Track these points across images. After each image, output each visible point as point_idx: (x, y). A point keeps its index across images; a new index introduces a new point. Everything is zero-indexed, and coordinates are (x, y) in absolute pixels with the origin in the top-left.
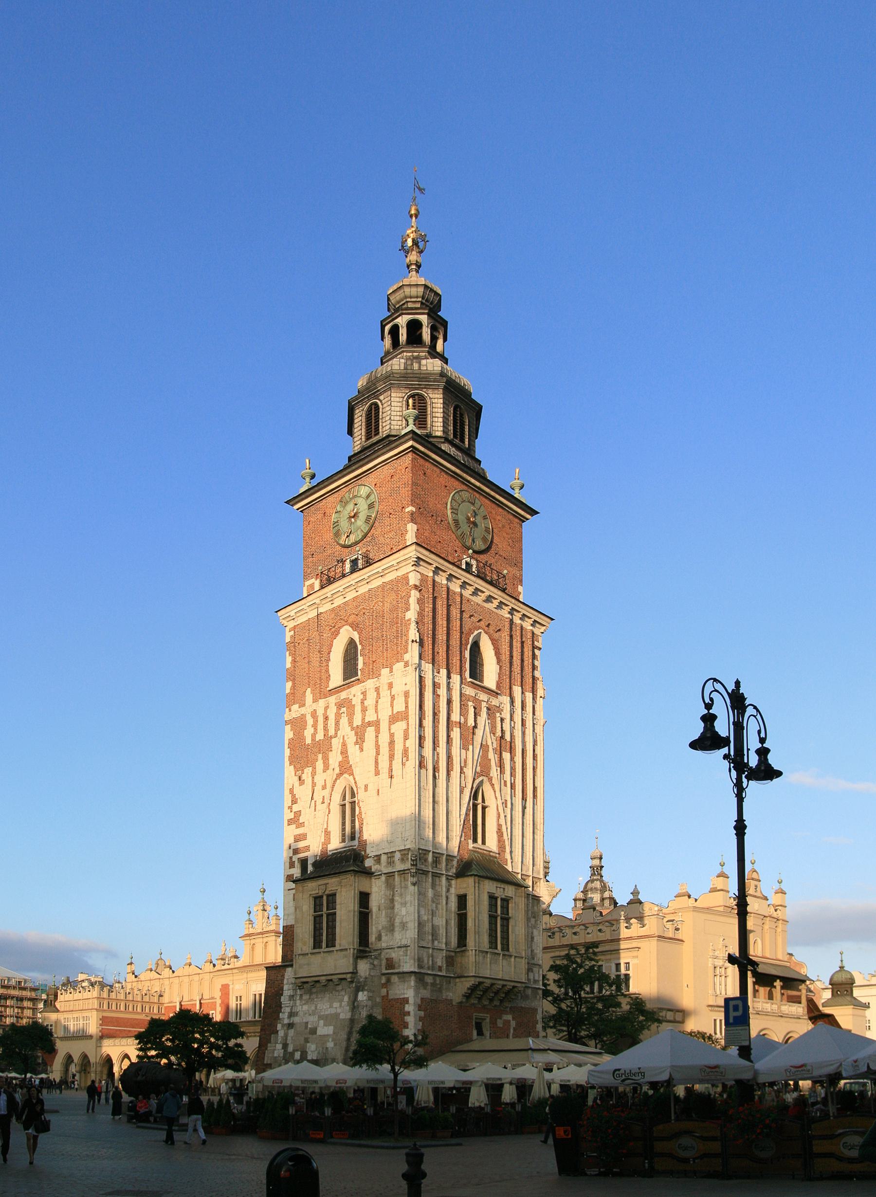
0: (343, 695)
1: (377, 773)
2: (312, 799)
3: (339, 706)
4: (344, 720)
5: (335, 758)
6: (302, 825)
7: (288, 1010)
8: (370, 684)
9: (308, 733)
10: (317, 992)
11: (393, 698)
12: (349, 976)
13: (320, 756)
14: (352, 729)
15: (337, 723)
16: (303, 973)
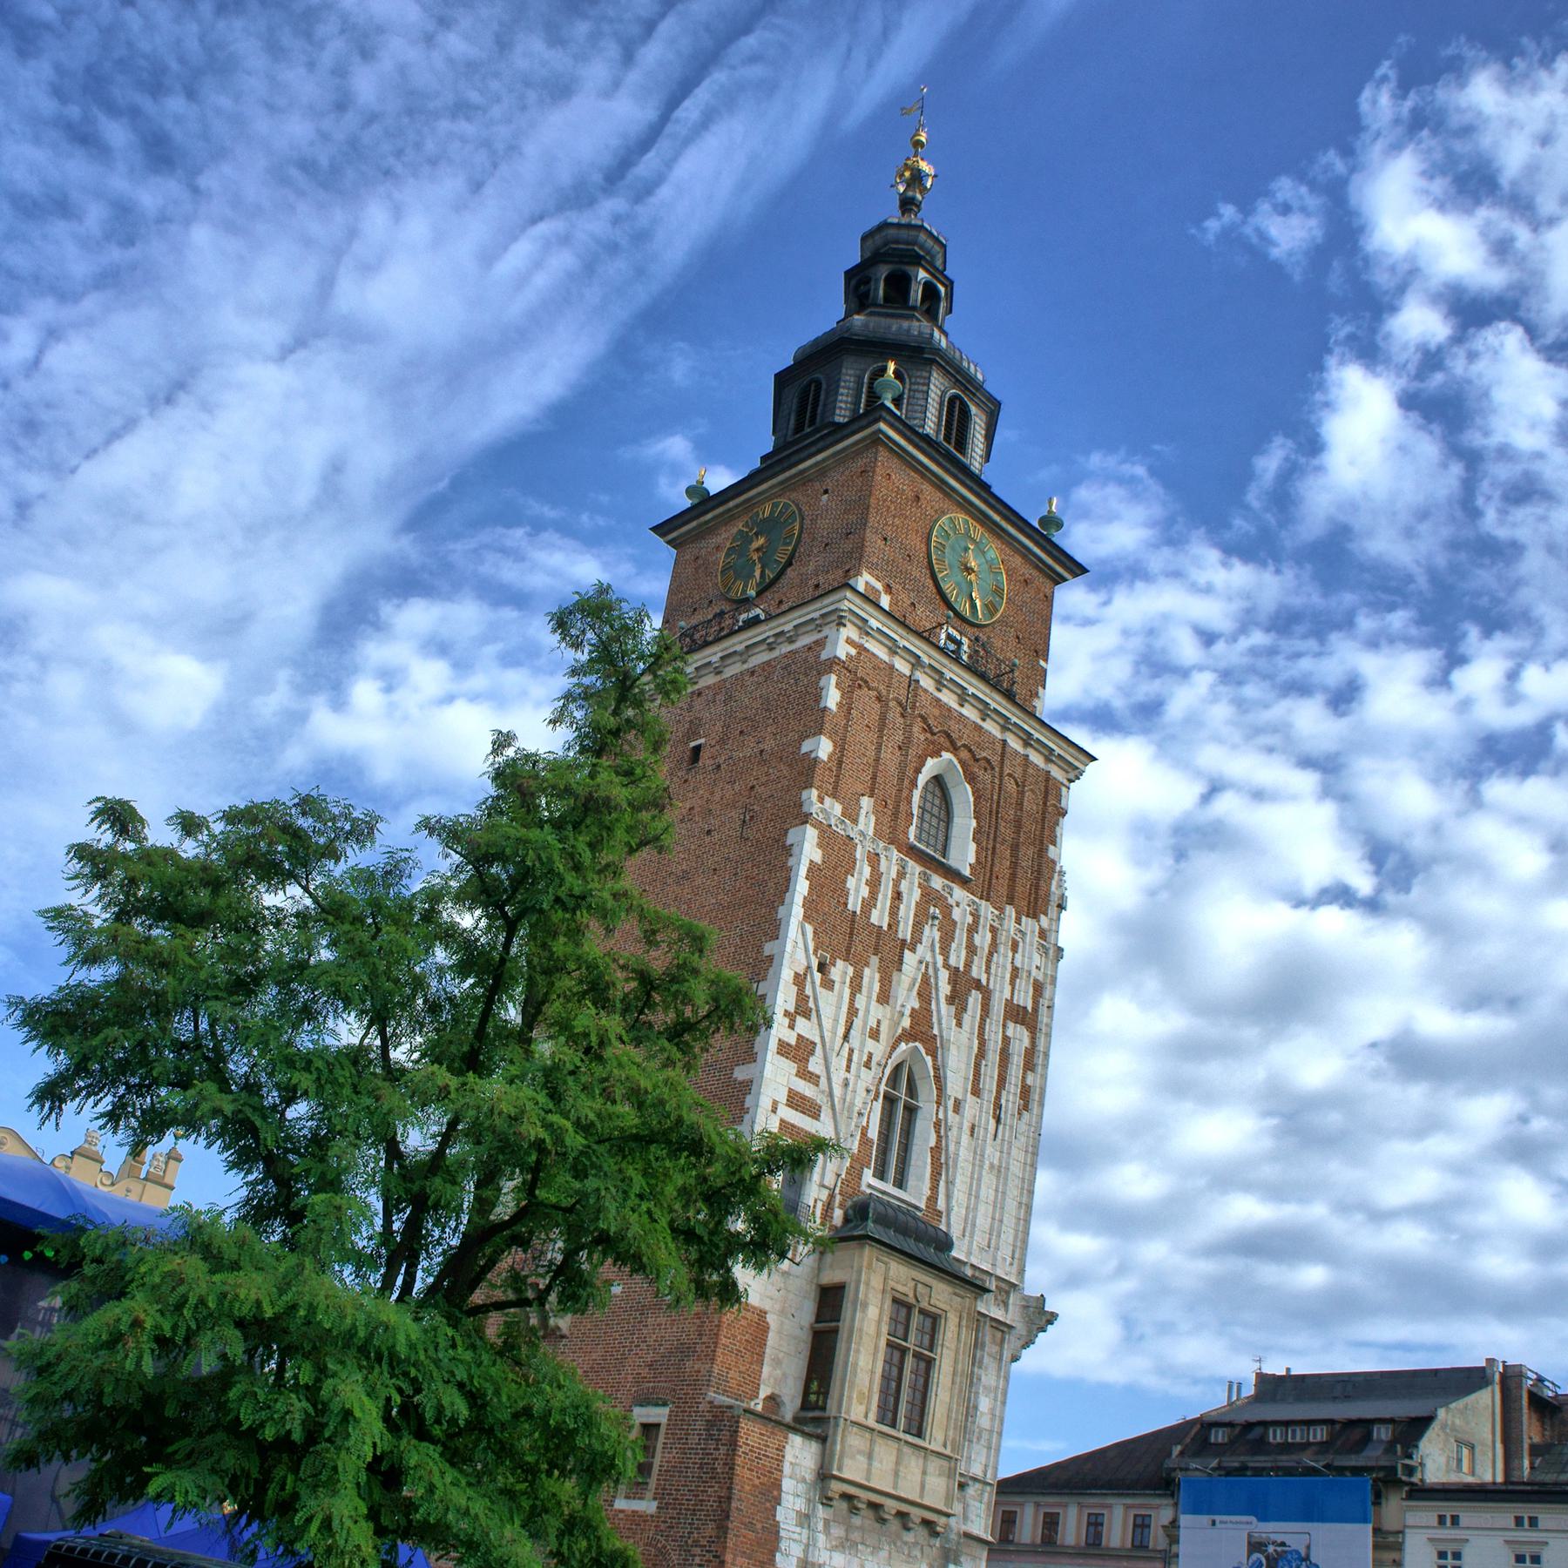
0: (937, 882)
1: (976, 1092)
2: (846, 1037)
3: (929, 896)
4: (931, 933)
5: (906, 998)
6: (813, 1078)
7: (797, 1551)
8: (987, 910)
9: (857, 888)
10: (862, 1528)
11: (1015, 972)
12: (942, 1520)
13: (875, 960)
14: (946, 966)
15: (918, 927)
16: (852, 1469)
